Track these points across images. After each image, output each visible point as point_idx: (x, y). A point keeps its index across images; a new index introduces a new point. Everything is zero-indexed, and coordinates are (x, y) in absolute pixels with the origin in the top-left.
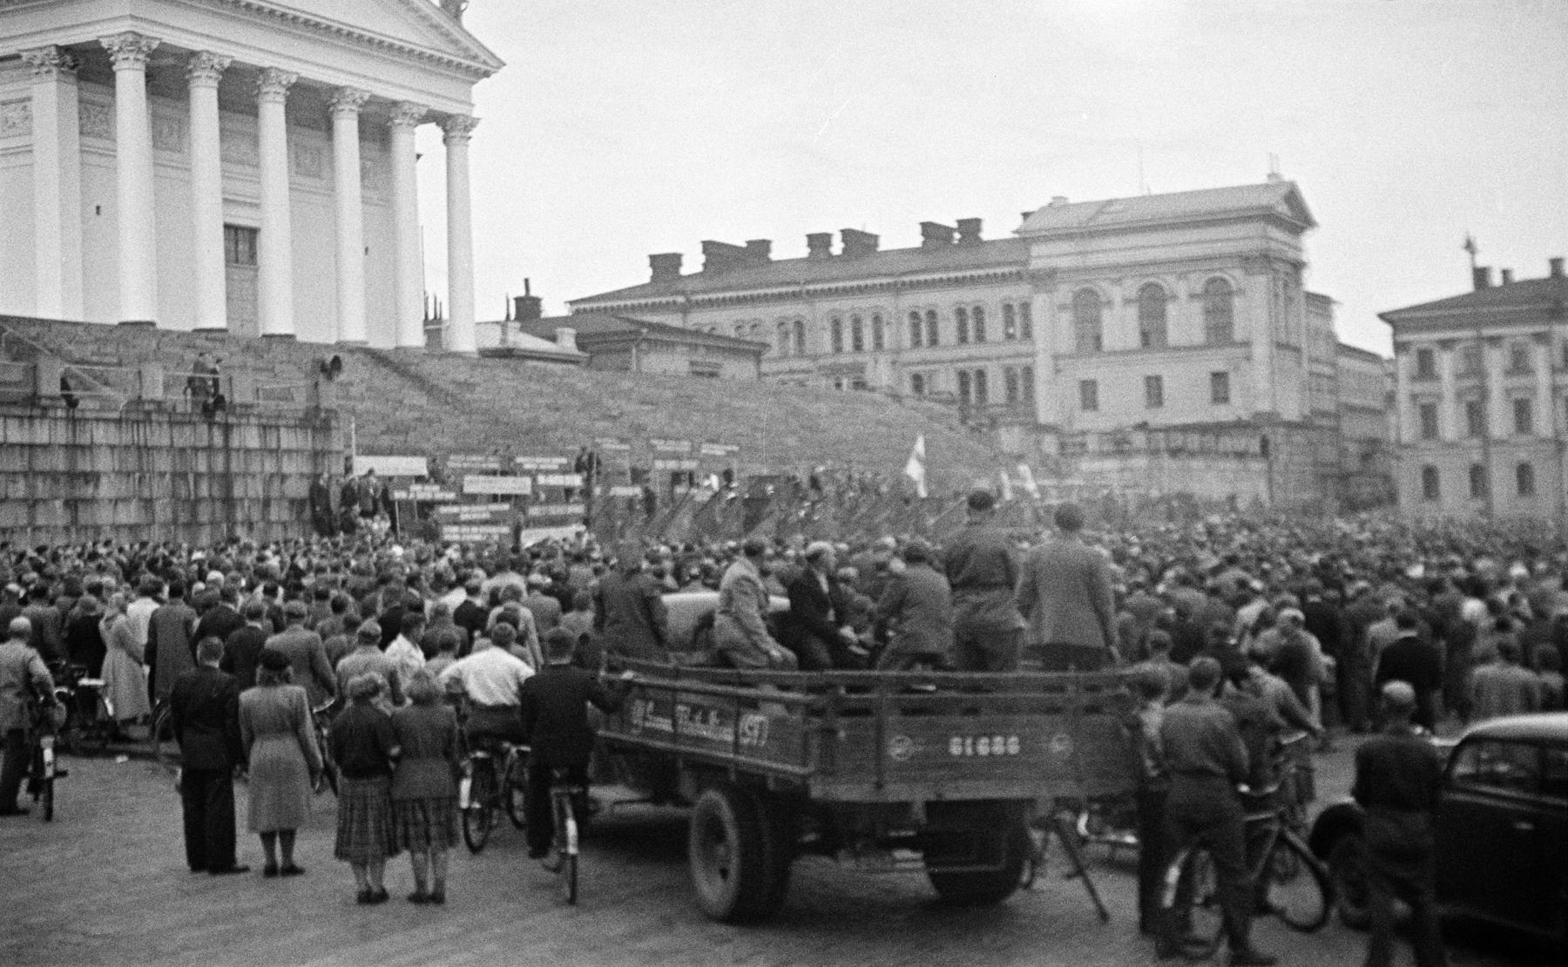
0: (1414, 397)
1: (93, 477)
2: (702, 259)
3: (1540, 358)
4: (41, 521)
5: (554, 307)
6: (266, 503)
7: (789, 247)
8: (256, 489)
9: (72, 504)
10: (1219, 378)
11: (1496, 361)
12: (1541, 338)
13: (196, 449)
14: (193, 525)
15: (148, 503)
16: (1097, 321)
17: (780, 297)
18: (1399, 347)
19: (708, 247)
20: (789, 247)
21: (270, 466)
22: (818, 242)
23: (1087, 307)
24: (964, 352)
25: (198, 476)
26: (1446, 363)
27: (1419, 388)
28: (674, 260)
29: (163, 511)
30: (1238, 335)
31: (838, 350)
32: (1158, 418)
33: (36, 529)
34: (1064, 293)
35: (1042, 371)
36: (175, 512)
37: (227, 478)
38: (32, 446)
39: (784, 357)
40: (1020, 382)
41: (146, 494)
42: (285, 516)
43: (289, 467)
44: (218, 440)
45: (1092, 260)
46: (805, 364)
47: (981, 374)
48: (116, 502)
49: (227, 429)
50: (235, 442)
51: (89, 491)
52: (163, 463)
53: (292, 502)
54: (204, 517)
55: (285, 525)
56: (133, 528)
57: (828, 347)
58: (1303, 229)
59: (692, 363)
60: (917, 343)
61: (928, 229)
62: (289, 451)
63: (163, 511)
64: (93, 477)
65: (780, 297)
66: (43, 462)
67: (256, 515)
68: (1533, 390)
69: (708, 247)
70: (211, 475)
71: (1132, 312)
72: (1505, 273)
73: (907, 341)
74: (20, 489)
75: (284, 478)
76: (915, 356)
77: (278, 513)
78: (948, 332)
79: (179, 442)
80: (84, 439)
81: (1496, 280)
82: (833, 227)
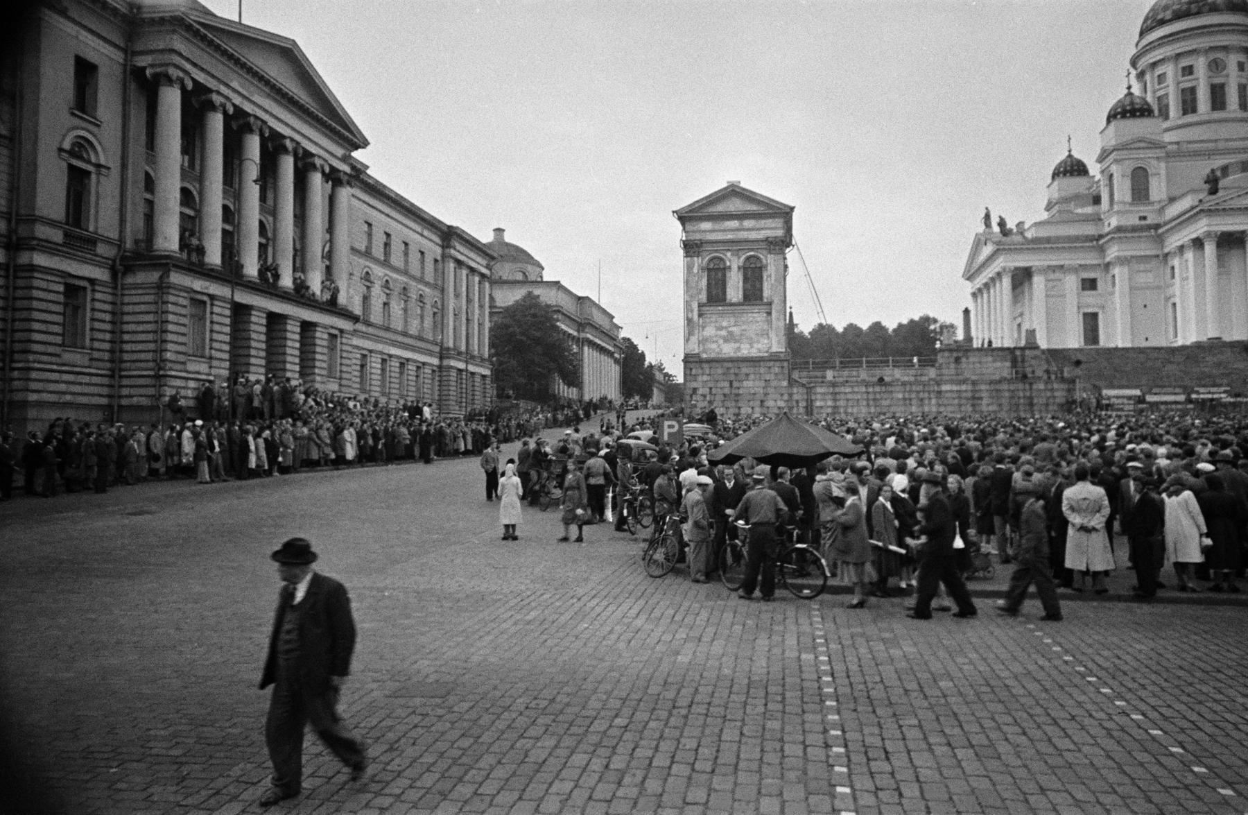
1: (981, 398)
6: (1047, 405)
9: (973, 405)
21: (1049, 394)
37: (1031, 398)
43: (1056, 394)
44: (1027, 387)
49: (1031, 384)
50: (1035, 387)
52: (1007, 394)
54: (1021, 408)
56: (995, 412)
64: (981, 398)
66: (964, 395)
67: (1043, 408)
74: (956, 401)
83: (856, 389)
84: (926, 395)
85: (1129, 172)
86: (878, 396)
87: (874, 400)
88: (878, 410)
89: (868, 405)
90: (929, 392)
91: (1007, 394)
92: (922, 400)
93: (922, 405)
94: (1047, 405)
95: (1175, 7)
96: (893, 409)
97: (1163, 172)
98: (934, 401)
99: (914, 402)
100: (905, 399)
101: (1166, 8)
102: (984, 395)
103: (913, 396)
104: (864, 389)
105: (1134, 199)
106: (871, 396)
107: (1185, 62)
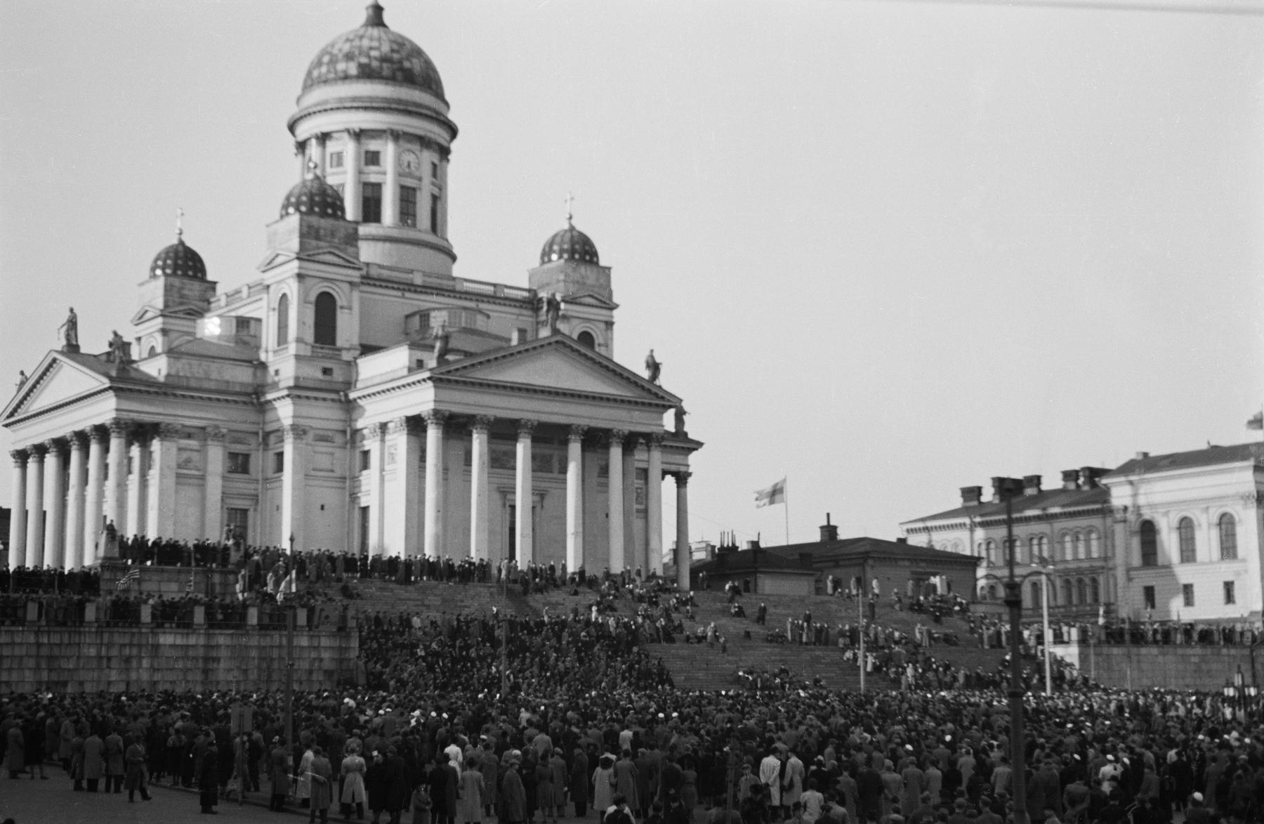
1: (217, 660)
4: (190, 678)
5: (843, 535)
6: (311, 672)
7: (1053, 482)
8: (305, 665)
9: (206, 671)
15: (245, 671)
20: (1053, 482)
21: (313, 655)
22: (1069, 475)
25: (272, 659)
28: (977, 491)
29: (253, 676)
33: (187, 682)
36: (259, 676)
38: (188, 646)
41: (244, 667)
42: (321, 678)
43: (326, 655)
44: (284, 642)
48: (229, 670)
51: (215, 665)
53: (326, 671)
55: (320, 683)
59: (913, 573)
62: (326, 648)
63: (253, 676)
64: (217, 660)
74: (180, 665)
75: (321, 660)
79: (263, 644)
80: (213, 642)
82: (1076, 466)
83: (18, 640)
84: (135, 651)
85: (313, 297)
86: (56, 652)
87: (51, 658)
88: (54, 677)
89: (38, 669)
90: (140, 646)
92: (128, 660)
93: (128, 670)
94: (311, 672)
95: (364, 60)
96: (83, 675)
97: (356, 306)
98: (145, 663)
99: (114, 663)
100: (100, 658)
101: (349, 57)
102: (223, 653)
103: (114, 652)
104: (32, 639)
105: (316, 341)
106: (44, 651)
107: (373, 145)
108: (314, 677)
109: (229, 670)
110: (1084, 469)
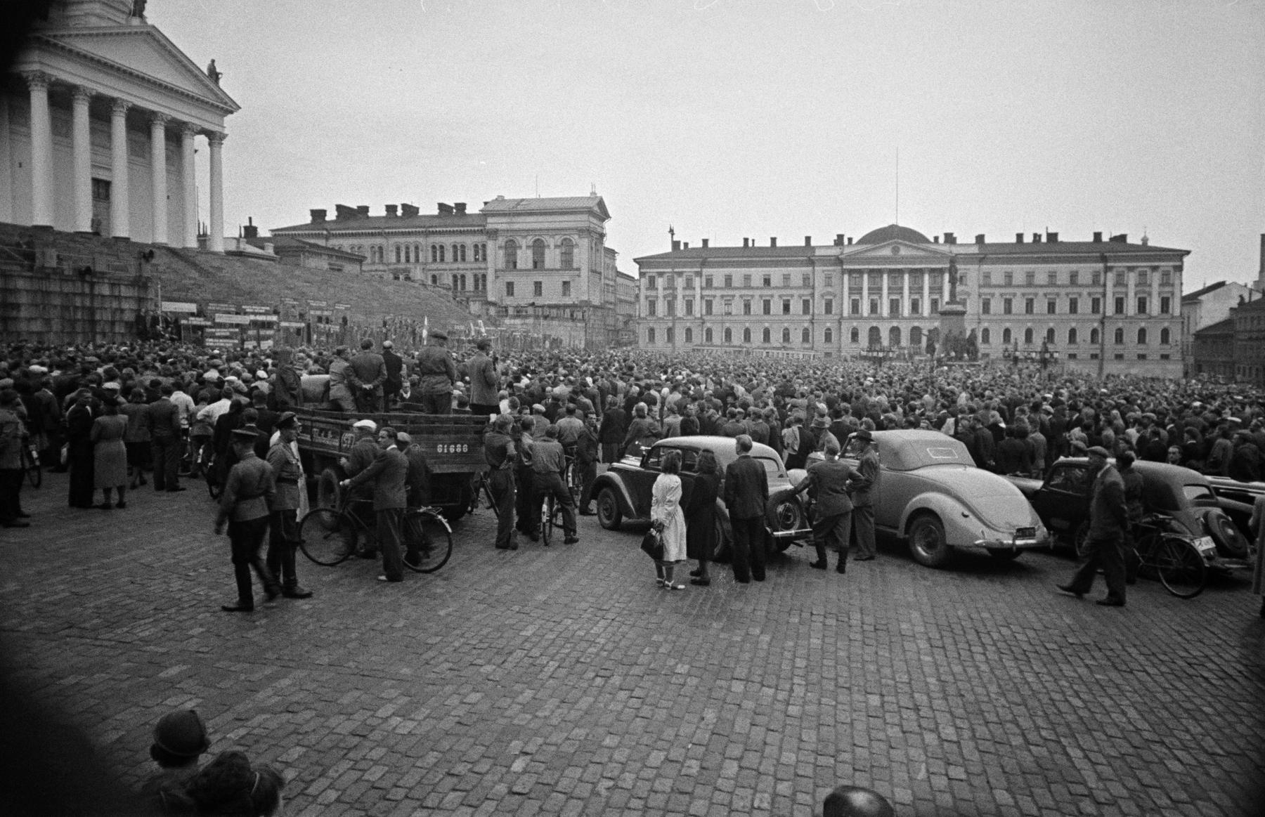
0: (647, 297)
1: (17, 307)
2: (336, 213)
3: (697, 282)
5: (263, 232)
6: (113, 323)
7: (377, 211)
8: (107, 316)
10: (565, 283)
11: (680, 283)
12: (699, 274)
13: (75, 294)
14: (73, 333)
15: (47, 321)
16: (515, 254)
17: (372, 234)
18: (642, 274)
19: (339, 208)
20: (377, 211)
21: (115, 305)
22: (391, 209)
23: (511, 249)
24: (455, 266)
25: (76, 308)
26: (660, 282)
27: (649, 293)
29: (56, 326)
30: (575, 266)
31: (399, 261)
32: (539, 301)
34: (501, 240)
35: (490, 278)
37: (92, 311)
39: (373, 263)
40: (480, 280)
43: (125, 306)
44: (87, 290)
45: (516, 227)
46: (381, 268)
47: (463, 277)
48: (30, 320)
49: (92, 285)
51: (14, 313)
52: (57, 301)
53: (127, 323)
55: (123, 335)
56: (39, 334)
57: (393, 259)
58: (603, 220)
60: (435, 260)
61: (442, 207)
63: (56, 326)
64: (17, 307)
65: (372, 234)
68: (694, 296)
69: (339, 208)
70: (83, 308)
71: (530, 253)
72: (686, 244)
73: (430, 260)
75: (122, 311)
76: (434, 266)
77: (119, 329)
78: (449, 256)
79: (66, 290)
80: (11, 286)
81: (682, 247)
82: (398, 203)
91: (57, 301)
94: (113, 323)
102: (23, 299)
108: (117, 329)
109: (30, 320)
110: (404, 206)
